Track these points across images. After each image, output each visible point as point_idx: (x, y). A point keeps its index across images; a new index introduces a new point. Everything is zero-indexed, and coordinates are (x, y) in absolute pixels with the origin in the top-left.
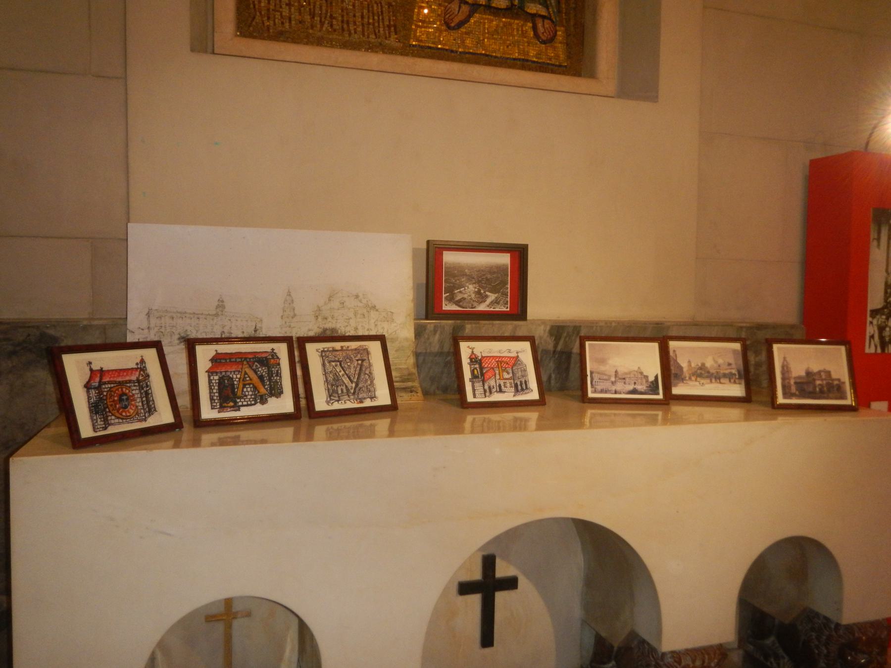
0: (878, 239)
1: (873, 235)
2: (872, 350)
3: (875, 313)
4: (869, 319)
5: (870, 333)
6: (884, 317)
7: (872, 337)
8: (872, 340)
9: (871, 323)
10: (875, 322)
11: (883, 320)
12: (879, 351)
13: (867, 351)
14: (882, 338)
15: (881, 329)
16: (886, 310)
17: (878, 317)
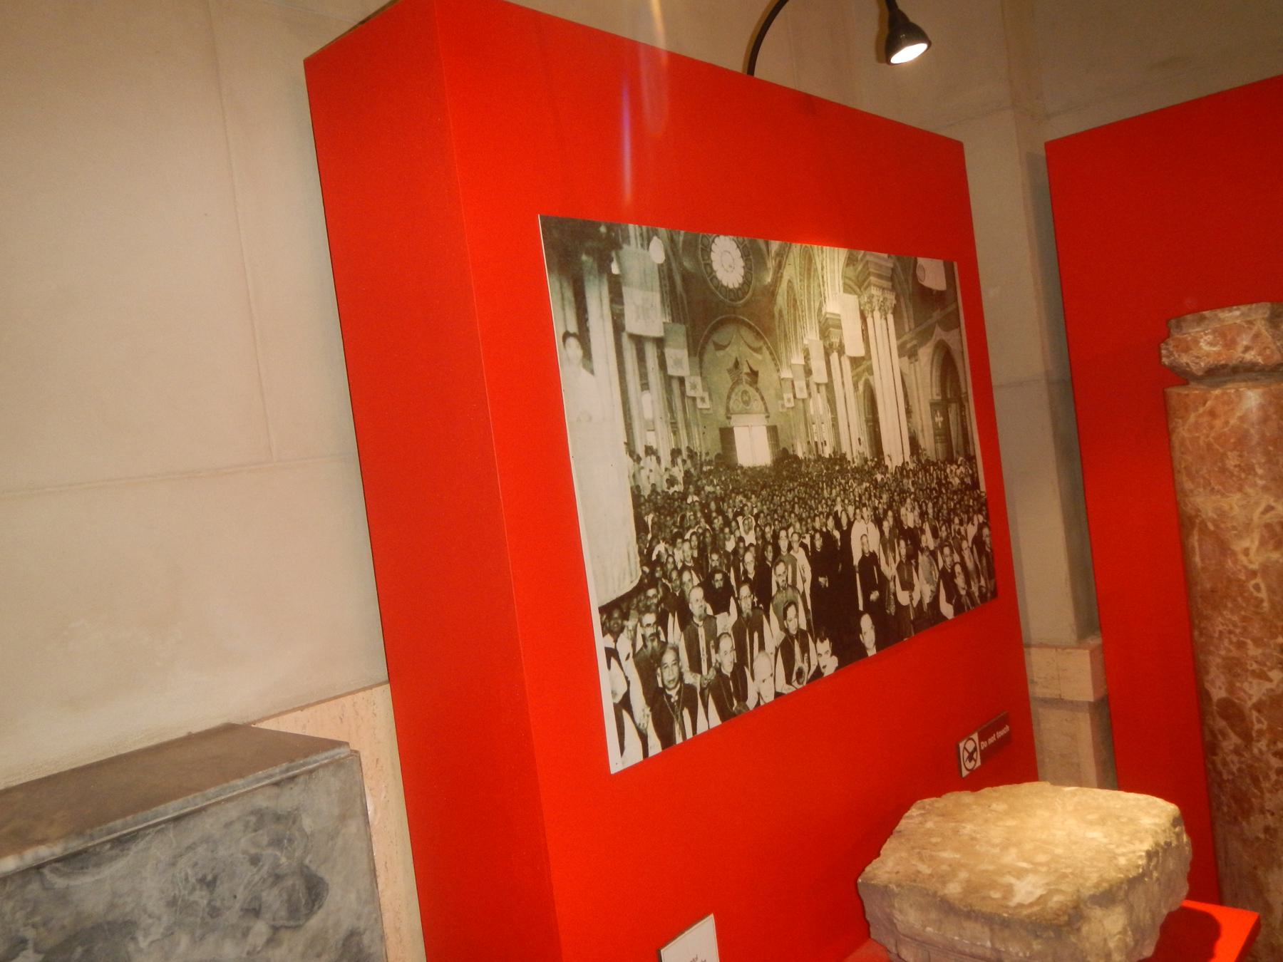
0: (583, 336)
1: (562, 319)
2: (634, 755)
3: (617, 610)
4: (602, 642)
5: (614, 694)
6: (650, 618)
7: (625, 704)
8: (625, 714)
9: (612, 653)
10: (624, 646)
11: (650, 631)
12: (655, 747)
13: (617, 764)
14: (655, 695)
15: (648, 666)
16: (651, 592)
17: (630, 624)
